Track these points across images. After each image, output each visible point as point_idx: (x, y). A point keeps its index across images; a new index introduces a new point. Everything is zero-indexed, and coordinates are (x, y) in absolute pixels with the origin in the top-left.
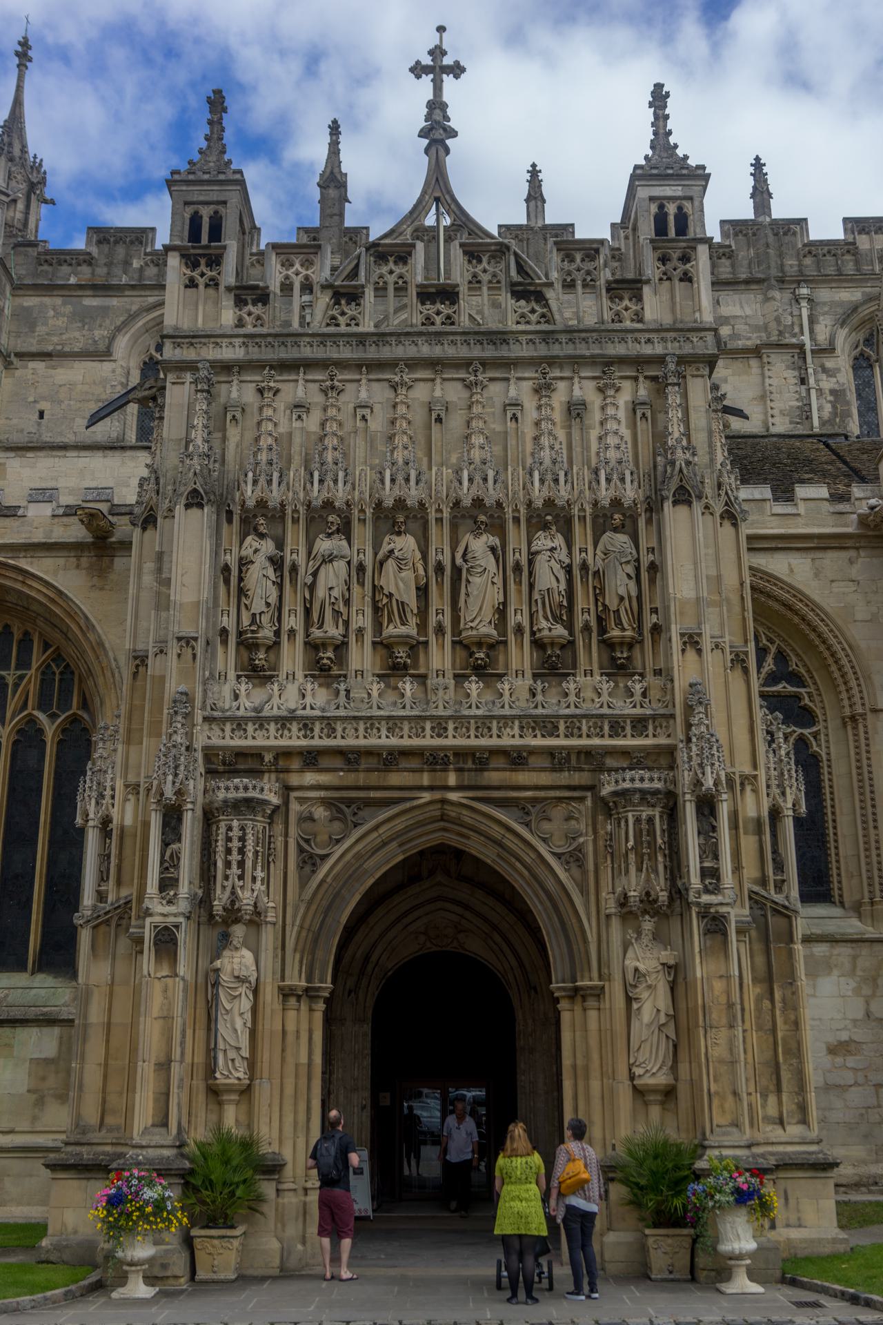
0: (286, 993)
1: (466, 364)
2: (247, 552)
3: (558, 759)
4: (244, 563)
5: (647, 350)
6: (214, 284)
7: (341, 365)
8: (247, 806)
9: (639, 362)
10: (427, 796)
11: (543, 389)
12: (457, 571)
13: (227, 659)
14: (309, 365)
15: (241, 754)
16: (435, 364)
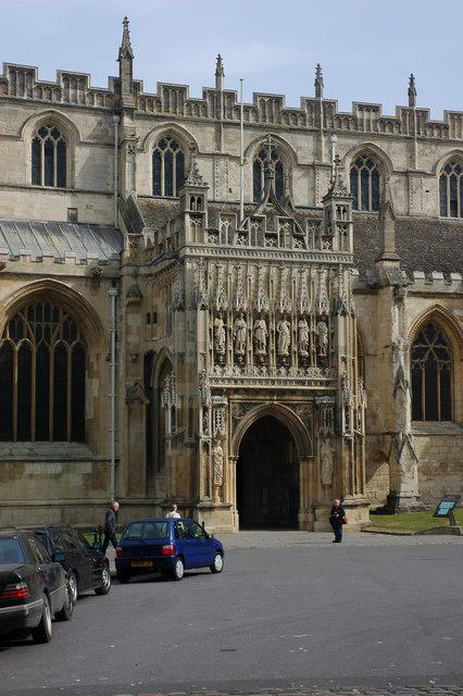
0: (230, 458)
1: (280, 262)
2: (216, 324)
3: (304, 392)
4: (215, 328)
5: (333, 261)
6: (201, 225)
7: (242, 260)
8: (222, 405)
9: (330, 265)
10: (268, 402)
11: (301, 272)
12: (277, 333)
13: (210, 359)
14: (232, 259)
15: (217, 389)
16: (270, 262)
